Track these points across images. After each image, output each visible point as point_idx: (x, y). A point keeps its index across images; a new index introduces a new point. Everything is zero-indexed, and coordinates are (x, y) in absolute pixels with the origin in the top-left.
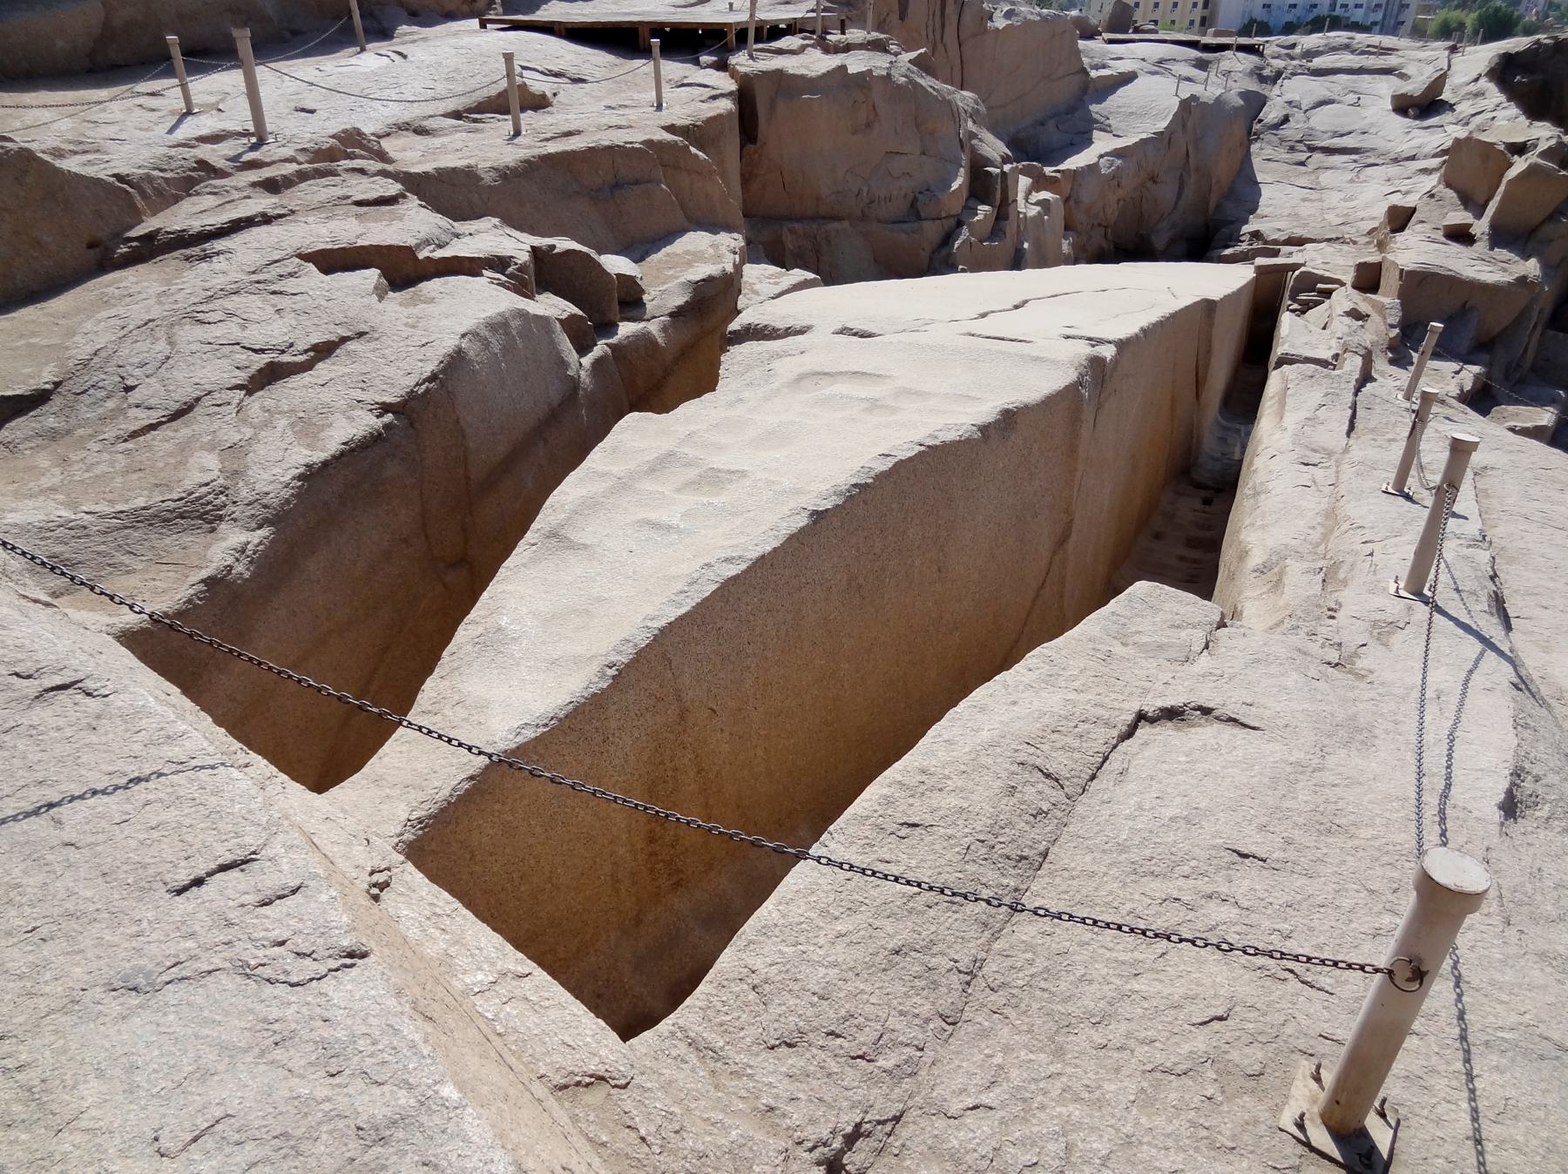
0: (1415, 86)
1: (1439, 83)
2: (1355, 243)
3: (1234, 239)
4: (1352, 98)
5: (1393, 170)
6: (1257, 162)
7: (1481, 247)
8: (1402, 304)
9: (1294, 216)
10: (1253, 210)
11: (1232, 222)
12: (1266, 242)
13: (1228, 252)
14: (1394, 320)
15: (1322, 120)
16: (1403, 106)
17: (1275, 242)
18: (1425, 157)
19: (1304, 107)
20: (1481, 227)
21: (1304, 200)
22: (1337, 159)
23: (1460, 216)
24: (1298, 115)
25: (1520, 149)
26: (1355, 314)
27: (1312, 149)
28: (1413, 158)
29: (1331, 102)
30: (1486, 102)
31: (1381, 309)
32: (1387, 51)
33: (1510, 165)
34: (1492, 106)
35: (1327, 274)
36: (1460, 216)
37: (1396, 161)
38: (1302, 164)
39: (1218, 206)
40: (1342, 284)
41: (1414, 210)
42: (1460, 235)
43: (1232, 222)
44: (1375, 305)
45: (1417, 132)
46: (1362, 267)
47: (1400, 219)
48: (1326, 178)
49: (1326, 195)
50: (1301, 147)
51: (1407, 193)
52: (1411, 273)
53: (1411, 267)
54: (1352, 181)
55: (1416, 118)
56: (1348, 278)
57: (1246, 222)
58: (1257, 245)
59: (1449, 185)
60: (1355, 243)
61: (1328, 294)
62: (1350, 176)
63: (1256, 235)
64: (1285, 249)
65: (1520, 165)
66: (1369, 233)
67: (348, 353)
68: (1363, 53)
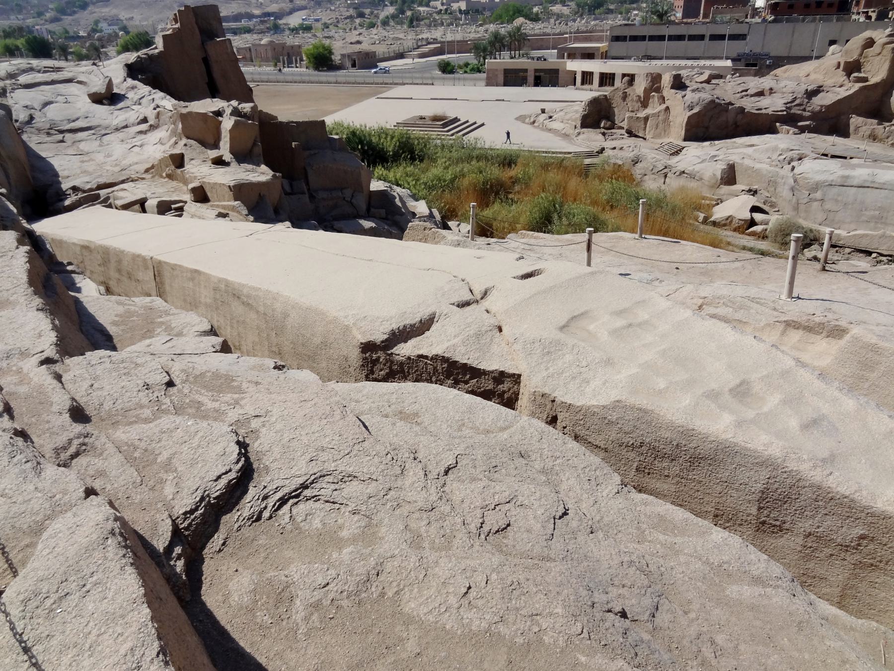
0: (99, 86)
1: (110, 84)
2: (143, 179)
3: (62, 195)
4: (59, 98)
5: (120, 135)
6: (32, 145)
7: (234, 164)
8: (242, 202)
9: (85, 172)
10: (56, 175)
11: (51, 185)
12: (84, 192)
13: (67, 203)
14: (245, 212)
15: (54, 113)
16: (97, 99)
17: (91, 190)
18: (133, 125)
19: (38, 109)
20: (228, 157)
21: (83, 162)
22: (80, 135)
23: (213, 154)
24: (37, 115)
25: (219, 113)
27: (61, 132)
28: (126, 127)
29: (51, 103)
30: (141, 91)
31: (233, 208)
32: (58, 69)
33: (221, 122)
34: (147, 93)
35: (173, 199)
36: (213, 154)
37: (117, 129)
38: (62, 141)
39: (33, 178)
40: (186, 202)
41: (182, 156)
42: (219, 162)
43: (51, 185)
44: (224, 207)
45: (116, 113)
46: (194, 190)
47: (179, 161)
48: (83, 146)
49: (92, 156)
50: (52, 132)
51: (141, 146)
52: (234, 186)
53: (232, 184)
54: (100, 146)
55: (110, 105)
56: (187, 197)
57: (60, 183)
58: (80, 195)
59: (188, 138)
60: (143, 179)
61: (181, 209)
62: (98, 142)
63: (75, 189)
64: (103, 193)
65: (227, 123)
66: (147, 171)
68: (45, 72)
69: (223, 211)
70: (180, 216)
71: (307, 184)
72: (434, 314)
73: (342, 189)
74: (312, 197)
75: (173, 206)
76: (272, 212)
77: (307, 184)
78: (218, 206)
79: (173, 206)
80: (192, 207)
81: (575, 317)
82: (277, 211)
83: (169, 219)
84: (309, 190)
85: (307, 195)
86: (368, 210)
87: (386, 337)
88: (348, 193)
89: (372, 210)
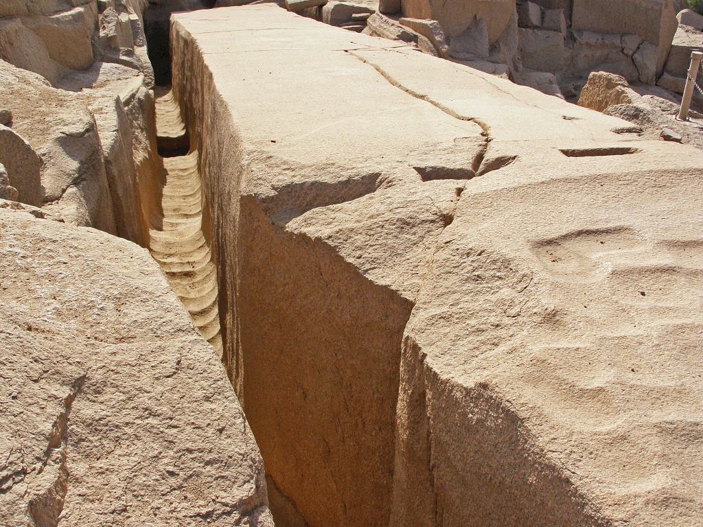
26: (405, 37)
44: (415, 26)
67: (93, 425)
69: (409, 30)
70: (359, 30)
71: (569, 17)
72: (376, 176)
73: (623, 35)
74: (571, 38)
75: (354, 15)
76: (487, 47)
77: (569, 17)
78: (408, 24)
79: (354, 15)
80: (377, 20)
81: (589, 232)
82: (494, 48)
83: (342, 34)
84: (569, 26)
85: (564, 33)
86: (659, 76)
87: (273, 193)
88: (631, 43)
89: (666, 76)
